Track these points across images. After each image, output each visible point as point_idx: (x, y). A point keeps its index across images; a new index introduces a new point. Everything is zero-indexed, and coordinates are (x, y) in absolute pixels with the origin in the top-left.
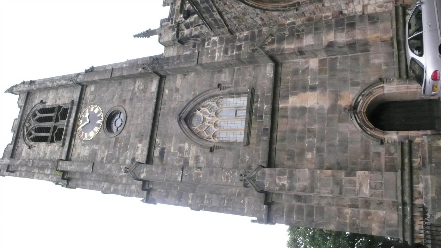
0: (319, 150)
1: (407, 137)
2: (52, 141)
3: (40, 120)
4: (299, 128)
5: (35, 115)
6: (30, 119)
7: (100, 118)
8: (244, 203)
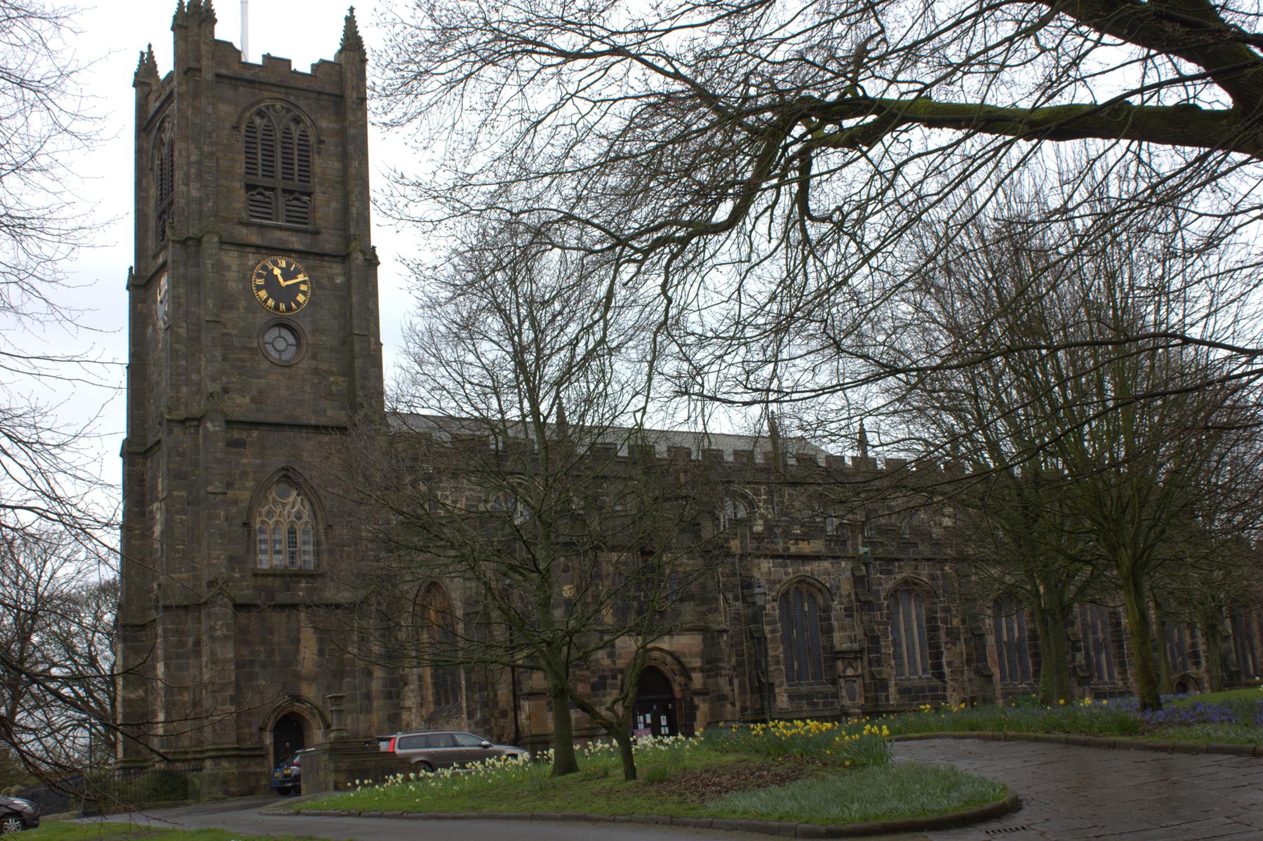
0: (252, 662)
1: (268, 754)
2: (250, 187)
3: (287, 131)
4: (276, 638)
5: (297, 121)
6: (288, 111)
7: (289, 309)
8: (181, 572)
